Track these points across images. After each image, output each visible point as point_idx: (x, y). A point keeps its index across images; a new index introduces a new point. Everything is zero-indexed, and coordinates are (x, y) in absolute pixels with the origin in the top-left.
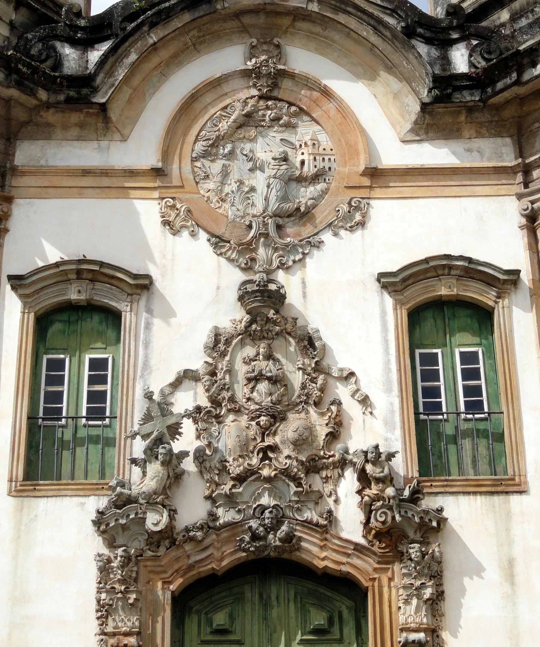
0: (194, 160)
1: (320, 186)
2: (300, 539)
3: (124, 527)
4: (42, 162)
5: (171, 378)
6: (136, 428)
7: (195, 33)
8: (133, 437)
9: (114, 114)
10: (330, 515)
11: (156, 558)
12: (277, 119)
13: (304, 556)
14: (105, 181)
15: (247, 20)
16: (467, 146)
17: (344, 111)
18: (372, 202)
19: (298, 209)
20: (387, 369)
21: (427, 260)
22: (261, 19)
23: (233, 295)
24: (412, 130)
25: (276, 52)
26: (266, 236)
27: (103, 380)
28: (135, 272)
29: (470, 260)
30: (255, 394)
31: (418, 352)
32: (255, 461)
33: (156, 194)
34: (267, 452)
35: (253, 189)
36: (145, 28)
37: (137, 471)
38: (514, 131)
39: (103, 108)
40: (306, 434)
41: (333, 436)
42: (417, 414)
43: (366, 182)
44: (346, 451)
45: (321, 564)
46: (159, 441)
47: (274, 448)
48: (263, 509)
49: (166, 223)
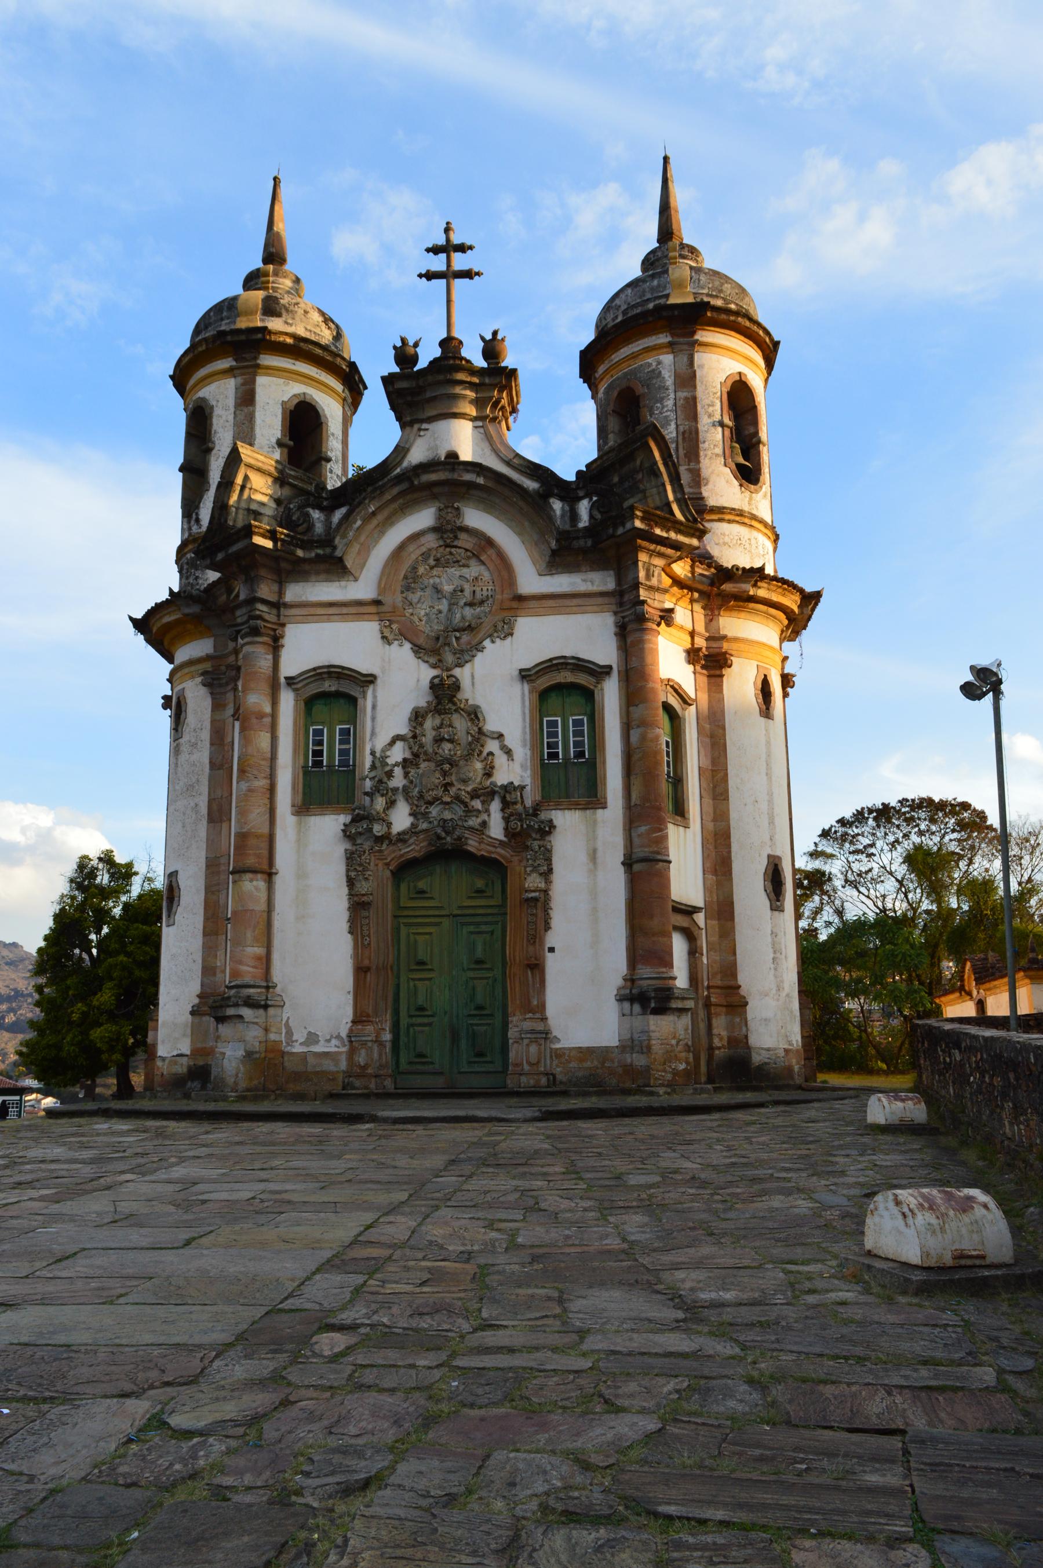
0: (402, 592)
1: (485, 608)
2: (467, 838)
3: (360, 834)
4: (304, 598)
5: (388, 740)
7: (401, 501)
8: (364, 779)
9: (349, 563)
10: (484, 824)
11: (381, 851)
12: (458, 561)
13: (469, 848)
14: (345, 610)
15: (436, 490)
16: (584, 577)
18: (519, 619)
19: (469, 626)
20: (524, 733)
21: (550, 660)
24: (547, 566)
25: (455, 513)
26: (449, 645)
28: (365, 672)
29: (578, 659)
30: (440, 751)
31: (545, 719)
32: (440, 792)
33: (376, 617)
34: (447, 786)
35: (440, 612)
37: (367, 799)
39: (341, 560)
40: (471, 775)
41: (488, 774)
42: (542, 759)
43: (515, 604)
44: (496, 786)
45: (479, 853)
46: (380, 781)
48: (445, 821)
49: (383, 637)
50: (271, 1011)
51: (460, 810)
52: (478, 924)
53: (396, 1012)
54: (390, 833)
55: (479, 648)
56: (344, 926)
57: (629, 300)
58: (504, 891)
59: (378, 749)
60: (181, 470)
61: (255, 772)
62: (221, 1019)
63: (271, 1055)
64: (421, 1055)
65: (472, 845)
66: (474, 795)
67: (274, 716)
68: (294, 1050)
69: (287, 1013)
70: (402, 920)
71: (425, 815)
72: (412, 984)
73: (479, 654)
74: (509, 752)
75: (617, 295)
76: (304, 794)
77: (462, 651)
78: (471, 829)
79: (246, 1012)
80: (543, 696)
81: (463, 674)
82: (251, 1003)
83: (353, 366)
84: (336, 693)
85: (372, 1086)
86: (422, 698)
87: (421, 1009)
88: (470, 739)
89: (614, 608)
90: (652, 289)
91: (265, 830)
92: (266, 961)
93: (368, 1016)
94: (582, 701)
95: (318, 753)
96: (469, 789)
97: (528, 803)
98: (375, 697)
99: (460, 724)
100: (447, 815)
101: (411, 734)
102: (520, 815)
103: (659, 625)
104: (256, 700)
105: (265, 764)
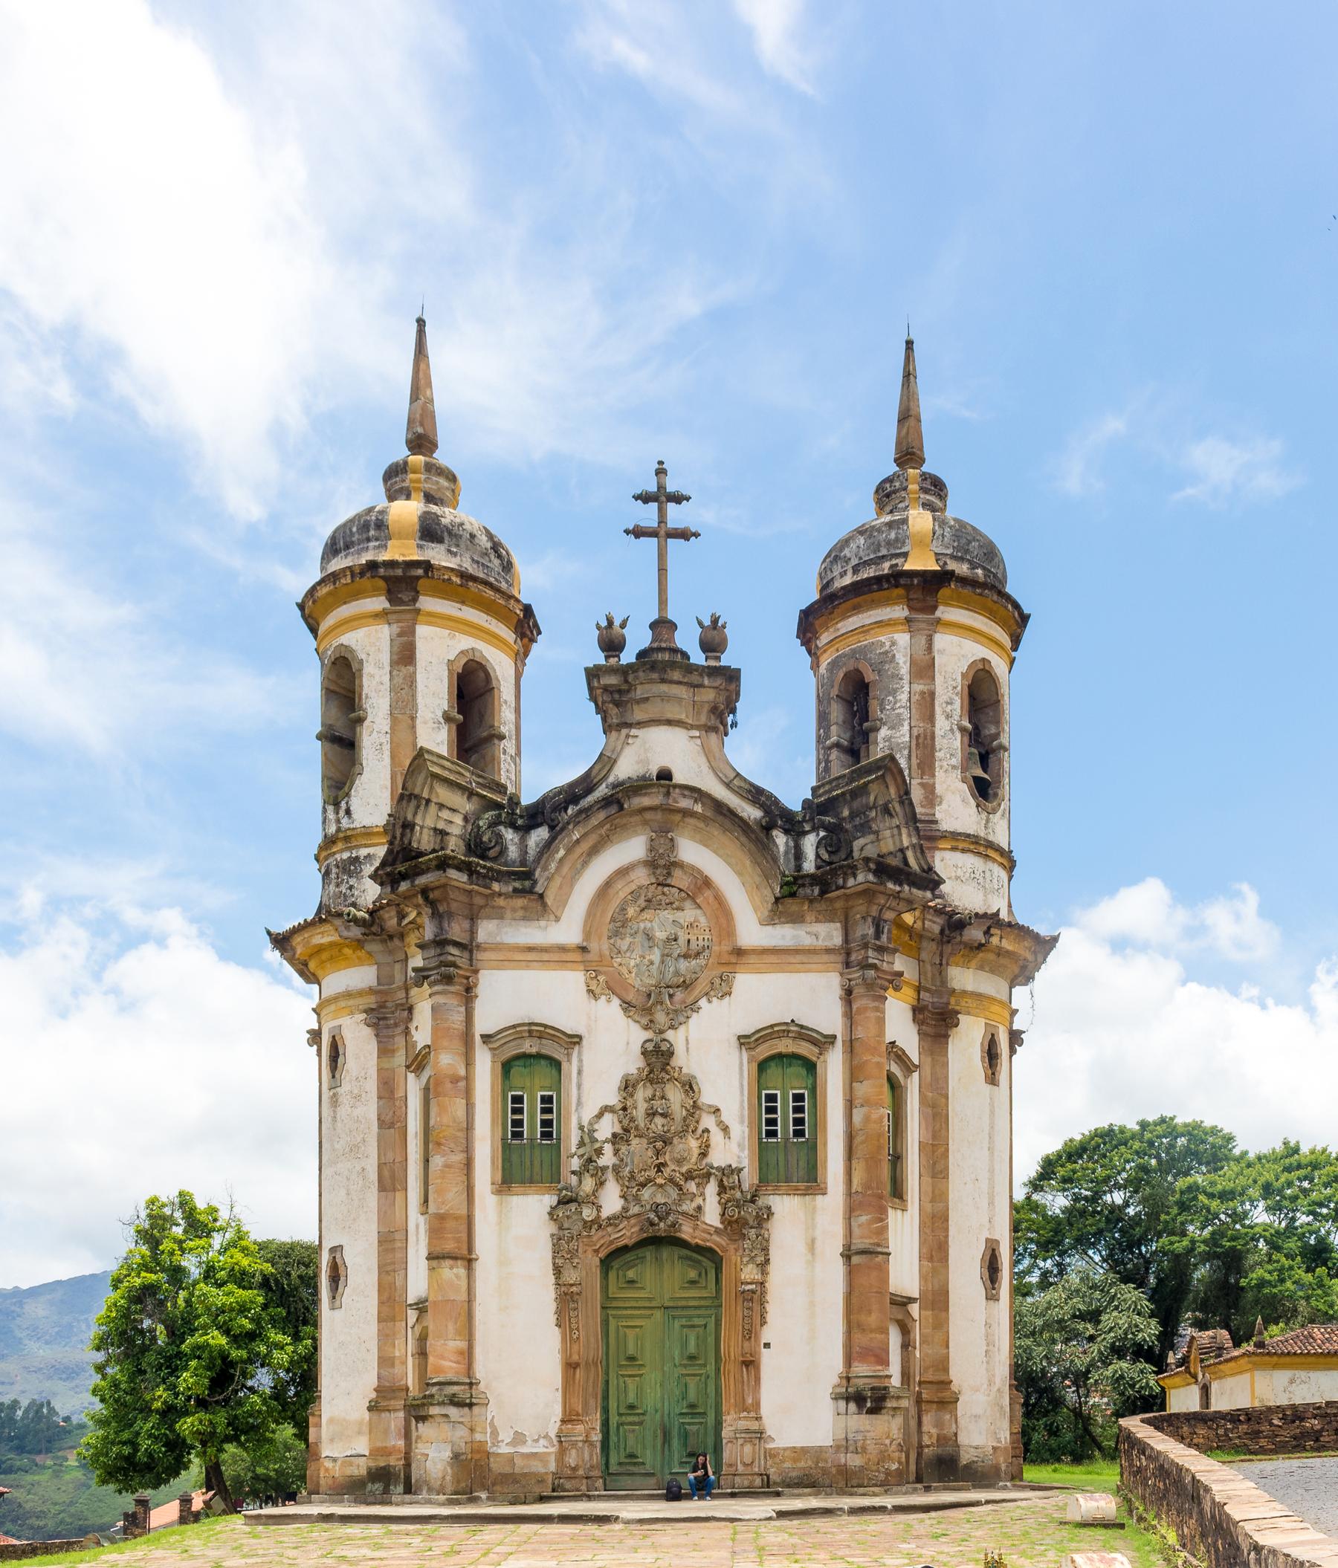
5: (596, 1112)
6: (574, 1150)
10: (699, 1208)
17: (720, 901)
21: (772, 1026)
22: (658, 816)
23: (638, 1050)
26: (662, 1003)
27: (550, 1111)
32: (652, 1173)
34: (660, 1168)
36: (571, 827)
37: (574, 1179)
38: (842, 918)
41: (704, 1155)
42: (760, 1139)
45: (693, 1241)
46: (590, 1160)
47: (664, 1165)
50: (476, 1409)
51: (674, 1193)
52: (690, 1317)
53: (605, 1410)
54: (598, 1217)
55: (693, 1007)
56: (553, 1318)
57: (861, 553)
58: (718, 1281)
59: (585, 1123)
60: (319, 737)
61: (452, 1145)
62: (423, 1419)
63: (477, 1456)
64: (632, 1456)
65: (686, 1232)
66: (689, 1176)
67: (468, 1079)
68: (500, 1451)
69: (492, 1411)
70: (610, 1312)
71: (637, 1199)
72: (621, 1380)
73: (695, 1015)
74: (725, 1130)
75: (845, 542)
76: (504, 1169)
77: (676, 1011)
78: (684, 1214)
79: (453, 1412)
80: (762, 1066)
81: (676, 1038)
82: (455, 1402)
83: (528, 610)
84: (535, 1058)
85: (584, 1488)
86: (633, 1064)
87: (632, 1407)
88: (684, 1113)
89: (839, 966)
90: (889, 544)
91: (464, 1212)
92: (468, 1356)
93: (578, 1415)
94: (804, 1072)
95: (517, 1123)
96: (684, 1170)
97: (746, 1186)
98: (580, 1061)
99: (675, 1096)
100: (660, 1199)
101: (620, 1106)
102: (738, 1201)
103: (886, 989)
104: (447, 1060)
105: (461, 1135)
